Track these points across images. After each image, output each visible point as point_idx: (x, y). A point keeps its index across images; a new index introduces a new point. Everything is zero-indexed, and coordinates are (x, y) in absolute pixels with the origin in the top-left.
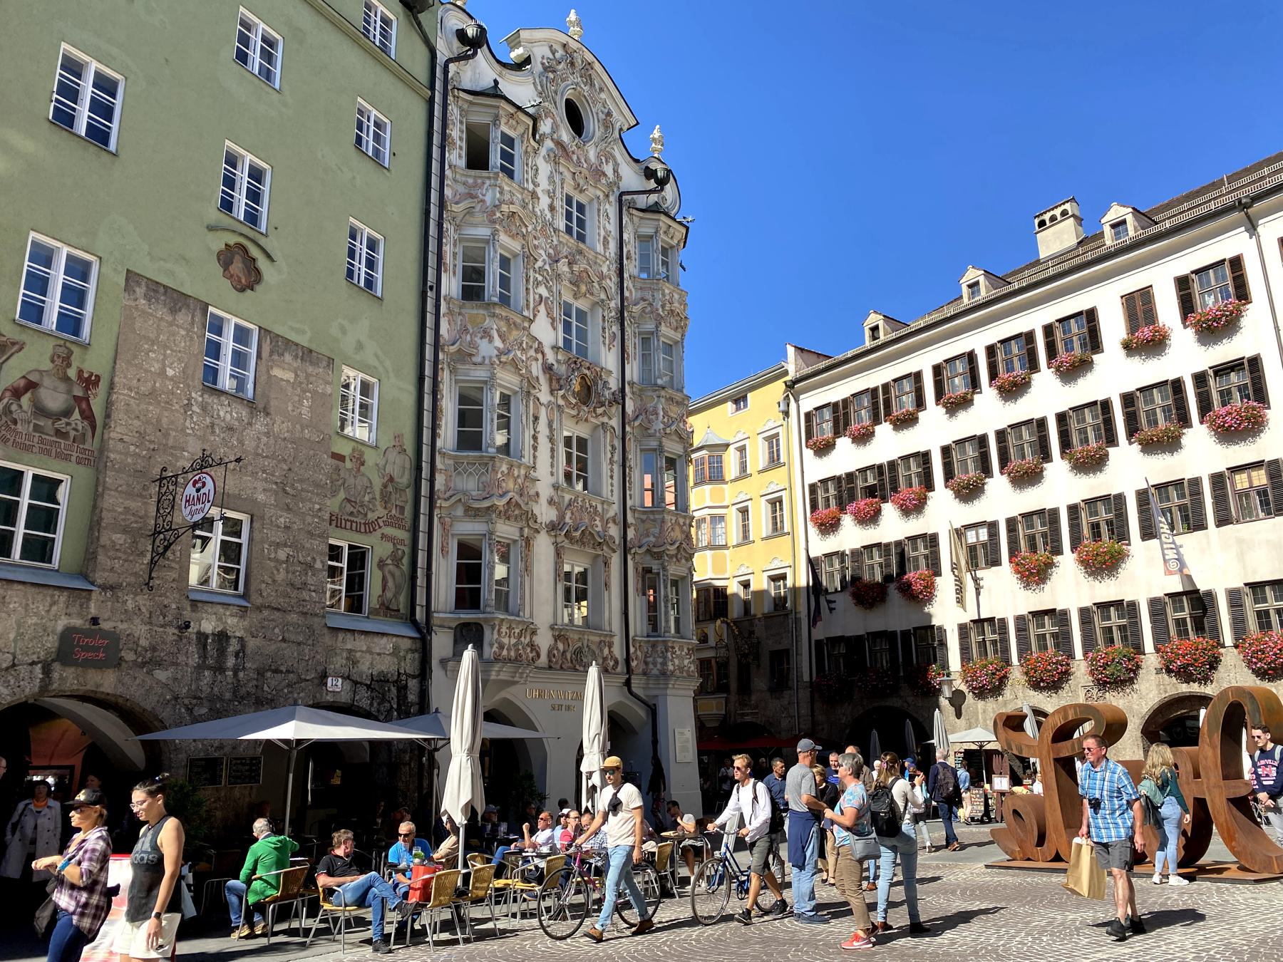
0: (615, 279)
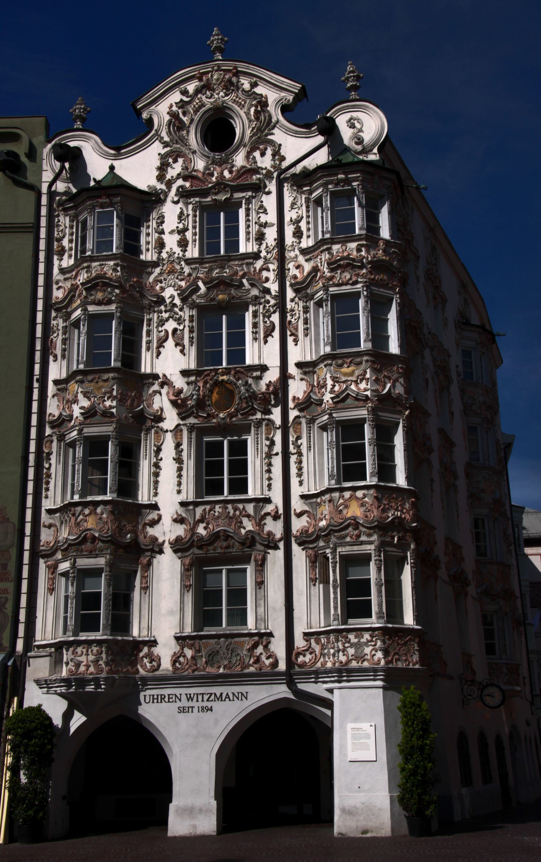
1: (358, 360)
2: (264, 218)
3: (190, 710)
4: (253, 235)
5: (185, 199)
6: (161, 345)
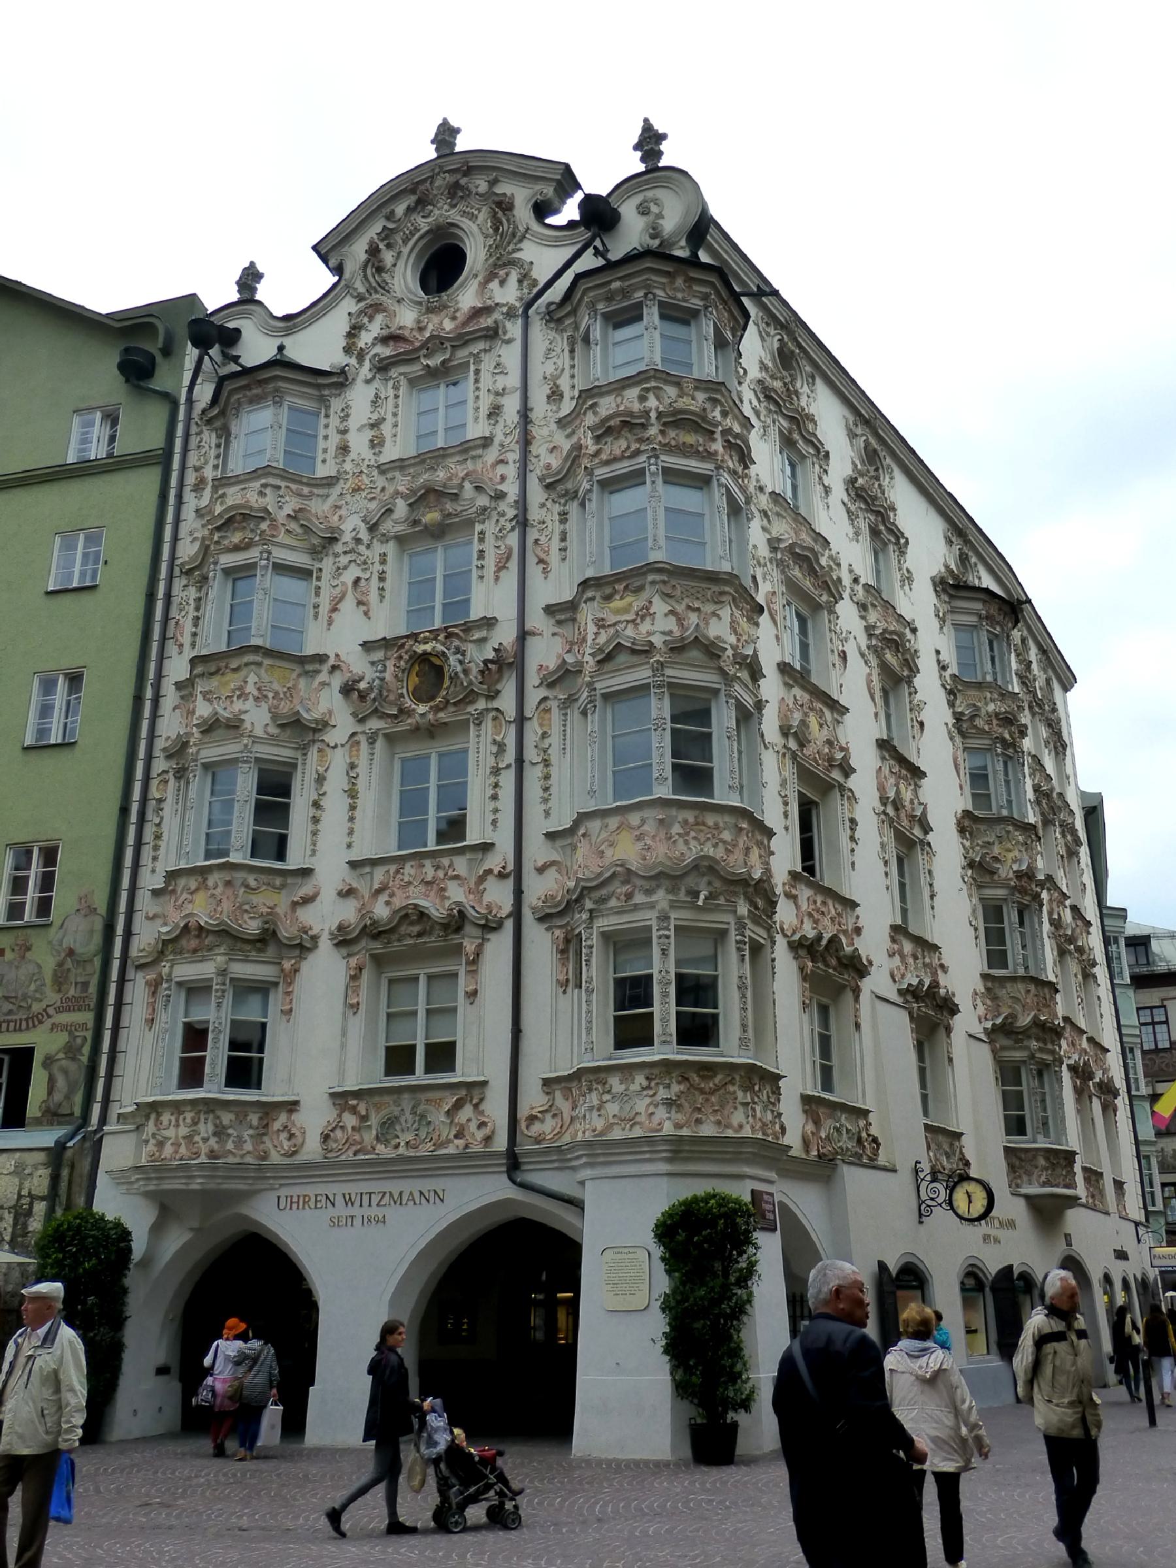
0: (513, 456)
3: (349, 1220)
6: (334, 609)
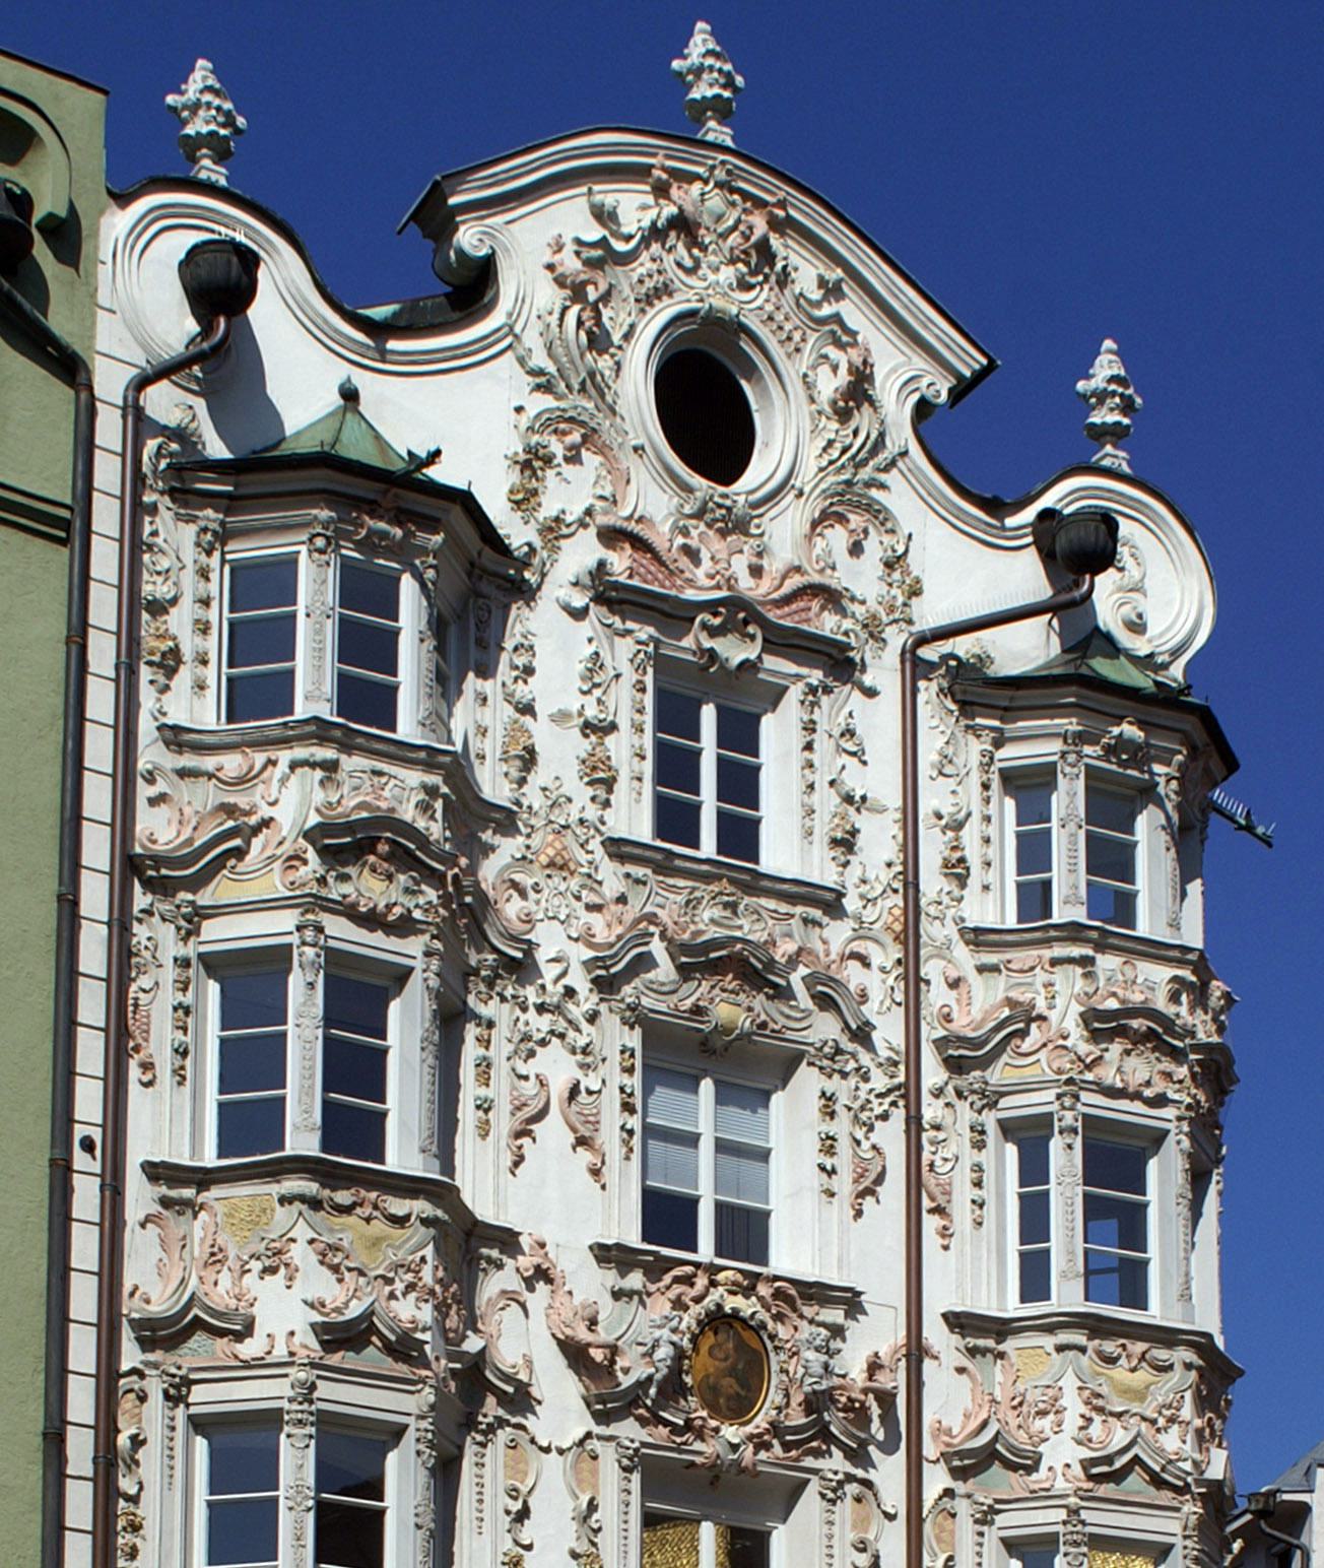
0: (885, 955)
1: (1162, 1354)
2: (856, 780)
4: (823, 826)
5: (604, 610)
